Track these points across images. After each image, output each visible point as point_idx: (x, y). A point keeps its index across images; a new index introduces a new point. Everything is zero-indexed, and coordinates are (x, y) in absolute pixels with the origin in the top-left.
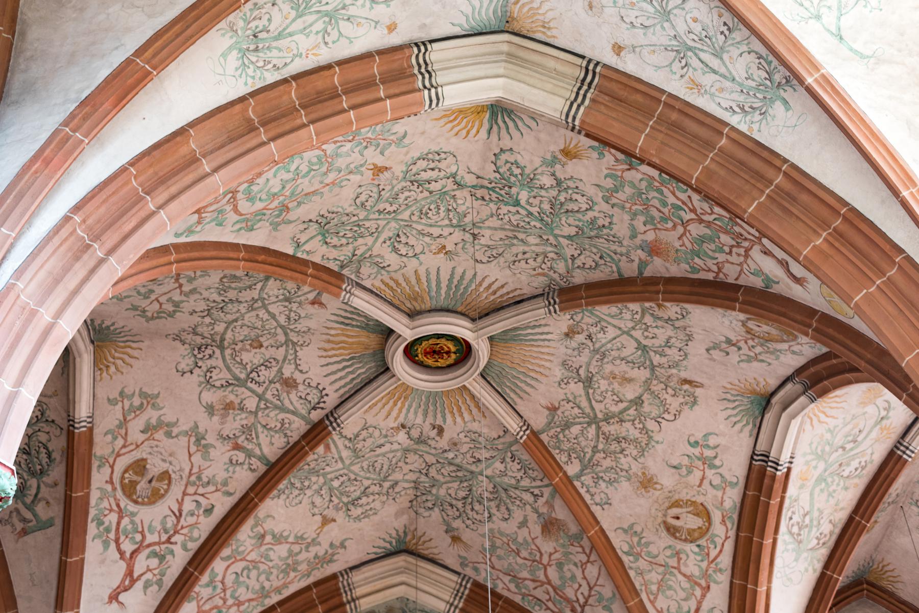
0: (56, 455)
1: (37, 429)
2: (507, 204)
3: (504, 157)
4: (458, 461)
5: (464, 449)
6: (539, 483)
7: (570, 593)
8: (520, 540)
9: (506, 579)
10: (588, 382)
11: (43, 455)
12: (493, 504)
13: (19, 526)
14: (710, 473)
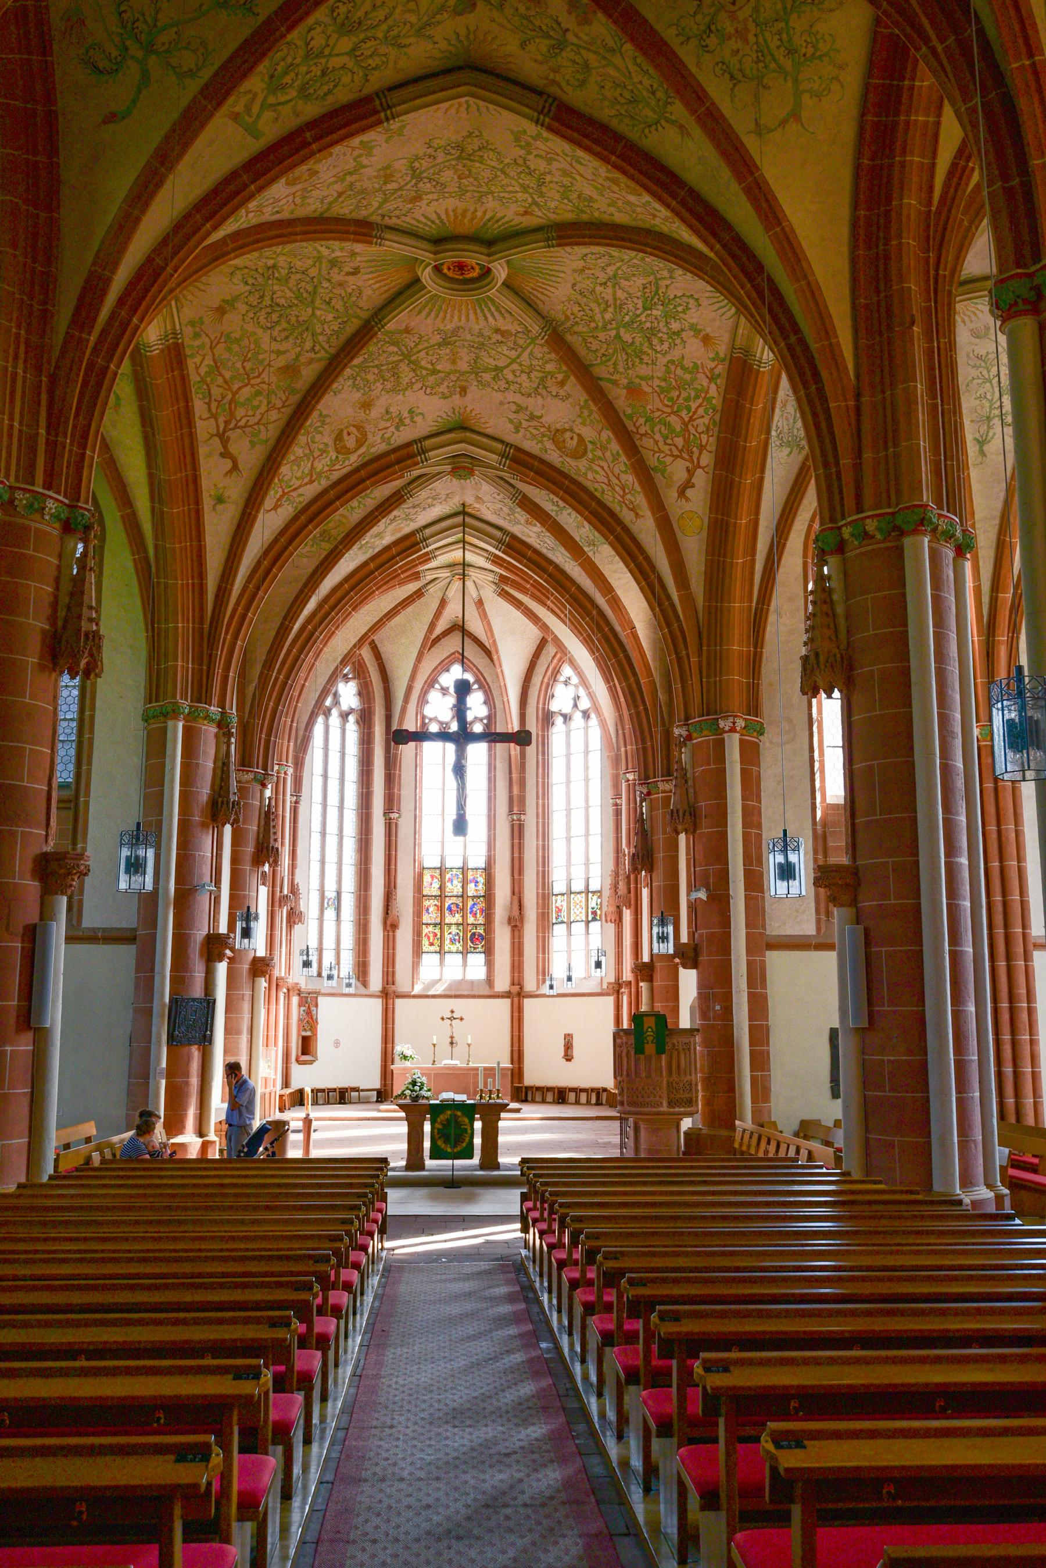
0: (330, 99)
1: (355, 69)
2: (644, 303)
3: (691, 301)
4: (320, 290)
5: (338, 291)
6: (326, 346)
7: (240, 412)
8: (260, 357)
9: (208, 361)
10: (445, 343)
11: (325, 88)
12: (285, 325)
13: (240, 108)
14: (392, 429)
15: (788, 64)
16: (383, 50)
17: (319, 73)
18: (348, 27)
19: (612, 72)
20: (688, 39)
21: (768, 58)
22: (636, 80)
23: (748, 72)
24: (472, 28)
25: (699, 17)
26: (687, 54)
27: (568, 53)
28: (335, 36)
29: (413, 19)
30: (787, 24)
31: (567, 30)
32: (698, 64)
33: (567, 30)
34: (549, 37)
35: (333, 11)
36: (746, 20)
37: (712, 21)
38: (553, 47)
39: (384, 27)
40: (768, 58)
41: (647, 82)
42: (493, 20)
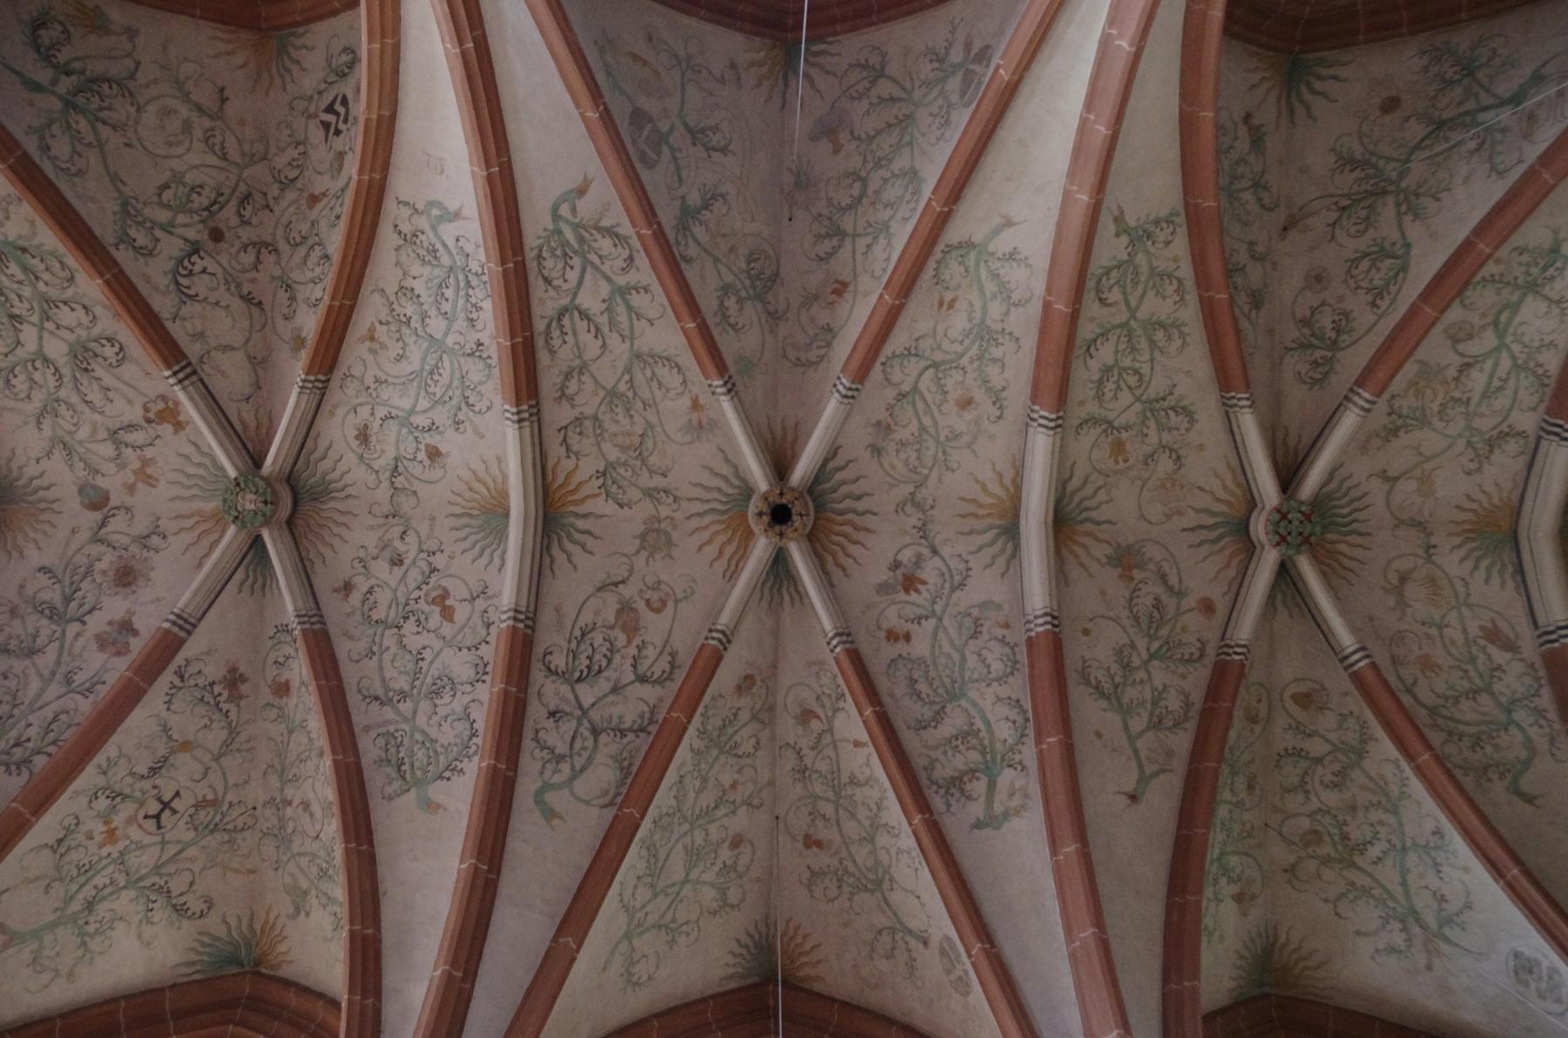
1: (11, 357)
15: (76, 906)
16: (38, 397)
17: (16, 311)
18: (83, 356)
19: (35, 684)
20: (105, 773)
21: (83, 879)
22: (31, 718)
23: (66, 859)
24: (56, 506)
25: (129, 780)
26: (89, 777)
27: (47, 628)
28: (71, 337)
29: (83, 434)
30: (124, 888)
31: (84, 623)
32: (77, 793)
33: (84, 623)
34: (68, 600)
35: (109, 340)
36: (127, 837)
37: (125, 797)
38: (53, 608)
39: (75, 399)
40: (83, 879)
41: (32, 732)
42: (74, 531)
